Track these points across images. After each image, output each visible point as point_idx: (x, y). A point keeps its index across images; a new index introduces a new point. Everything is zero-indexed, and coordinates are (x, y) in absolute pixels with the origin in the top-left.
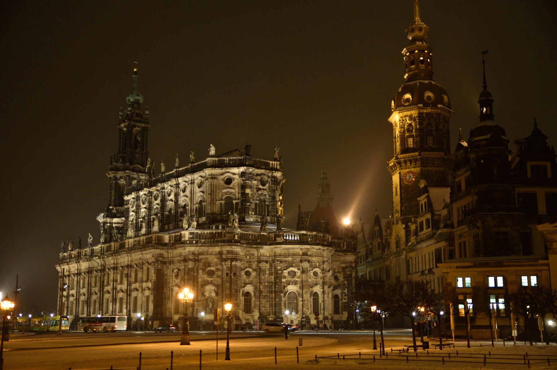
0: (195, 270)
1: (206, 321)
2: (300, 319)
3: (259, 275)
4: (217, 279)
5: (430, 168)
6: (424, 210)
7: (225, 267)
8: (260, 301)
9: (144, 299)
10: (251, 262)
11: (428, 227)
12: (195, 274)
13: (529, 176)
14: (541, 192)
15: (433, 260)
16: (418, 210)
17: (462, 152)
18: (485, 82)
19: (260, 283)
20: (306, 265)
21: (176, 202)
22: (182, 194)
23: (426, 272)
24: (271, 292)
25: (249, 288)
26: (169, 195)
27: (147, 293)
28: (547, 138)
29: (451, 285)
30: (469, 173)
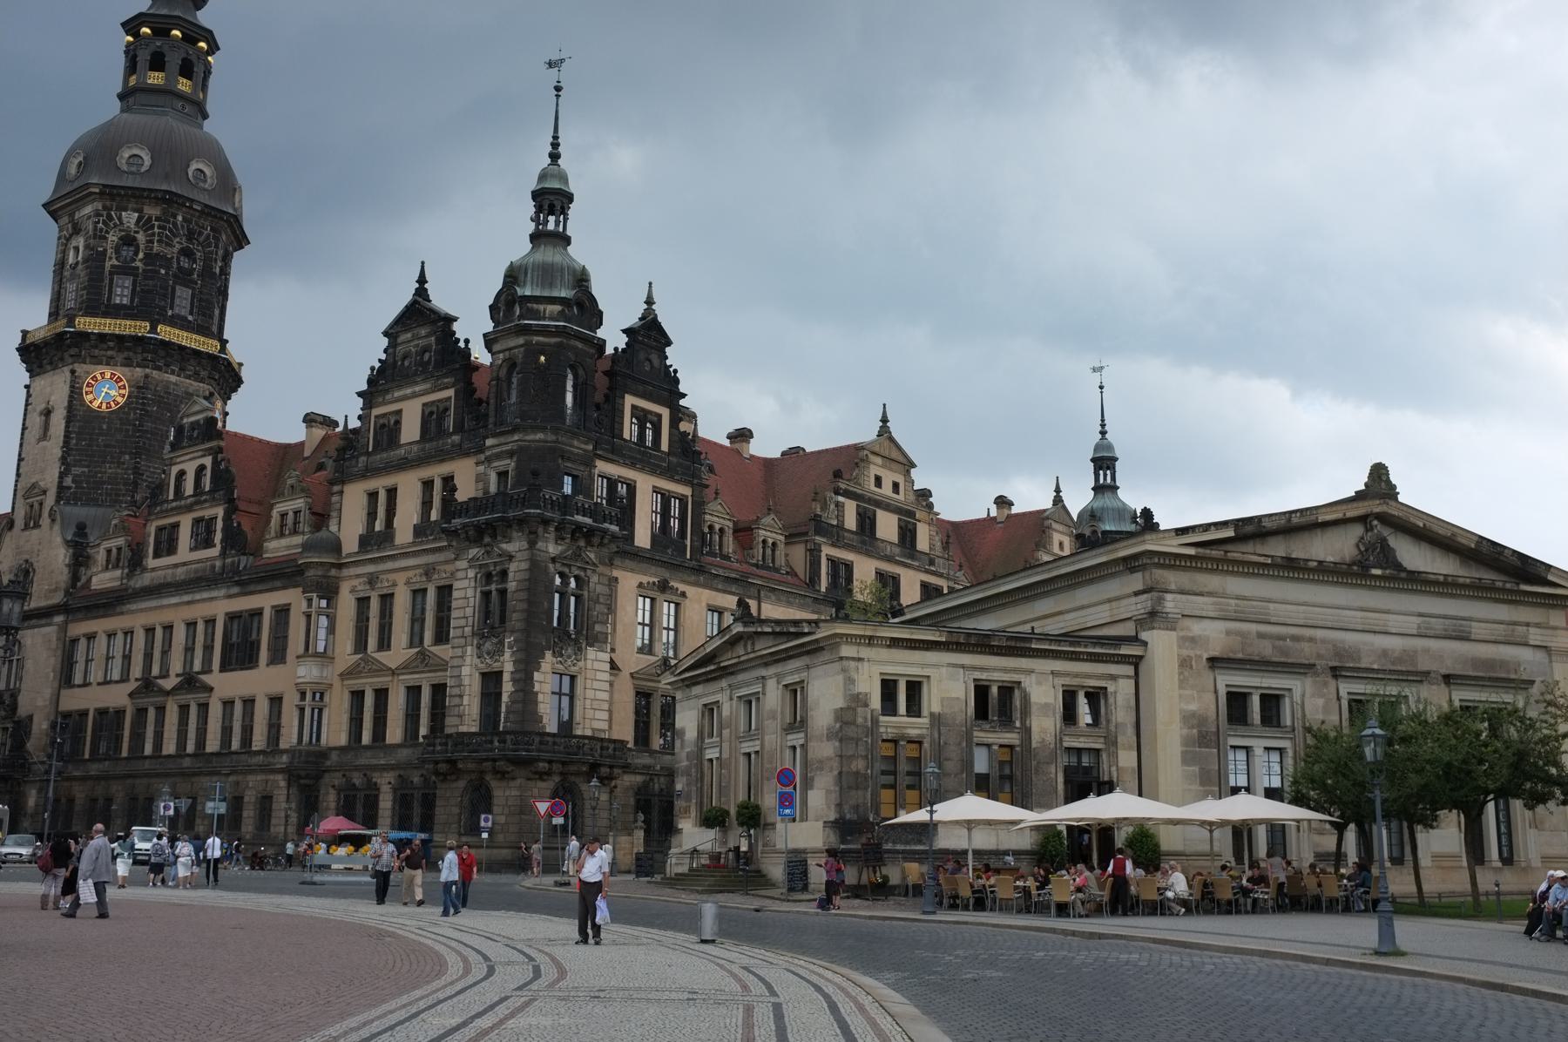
5: (173, 378)
6: (189, 488)
14: (646, 485)
15: (208, 648)
16: (160, 487)
17: (423, 332)
23: (168, 684)
28: (669, 343)
29: (866, 705)
30: (450, 393)
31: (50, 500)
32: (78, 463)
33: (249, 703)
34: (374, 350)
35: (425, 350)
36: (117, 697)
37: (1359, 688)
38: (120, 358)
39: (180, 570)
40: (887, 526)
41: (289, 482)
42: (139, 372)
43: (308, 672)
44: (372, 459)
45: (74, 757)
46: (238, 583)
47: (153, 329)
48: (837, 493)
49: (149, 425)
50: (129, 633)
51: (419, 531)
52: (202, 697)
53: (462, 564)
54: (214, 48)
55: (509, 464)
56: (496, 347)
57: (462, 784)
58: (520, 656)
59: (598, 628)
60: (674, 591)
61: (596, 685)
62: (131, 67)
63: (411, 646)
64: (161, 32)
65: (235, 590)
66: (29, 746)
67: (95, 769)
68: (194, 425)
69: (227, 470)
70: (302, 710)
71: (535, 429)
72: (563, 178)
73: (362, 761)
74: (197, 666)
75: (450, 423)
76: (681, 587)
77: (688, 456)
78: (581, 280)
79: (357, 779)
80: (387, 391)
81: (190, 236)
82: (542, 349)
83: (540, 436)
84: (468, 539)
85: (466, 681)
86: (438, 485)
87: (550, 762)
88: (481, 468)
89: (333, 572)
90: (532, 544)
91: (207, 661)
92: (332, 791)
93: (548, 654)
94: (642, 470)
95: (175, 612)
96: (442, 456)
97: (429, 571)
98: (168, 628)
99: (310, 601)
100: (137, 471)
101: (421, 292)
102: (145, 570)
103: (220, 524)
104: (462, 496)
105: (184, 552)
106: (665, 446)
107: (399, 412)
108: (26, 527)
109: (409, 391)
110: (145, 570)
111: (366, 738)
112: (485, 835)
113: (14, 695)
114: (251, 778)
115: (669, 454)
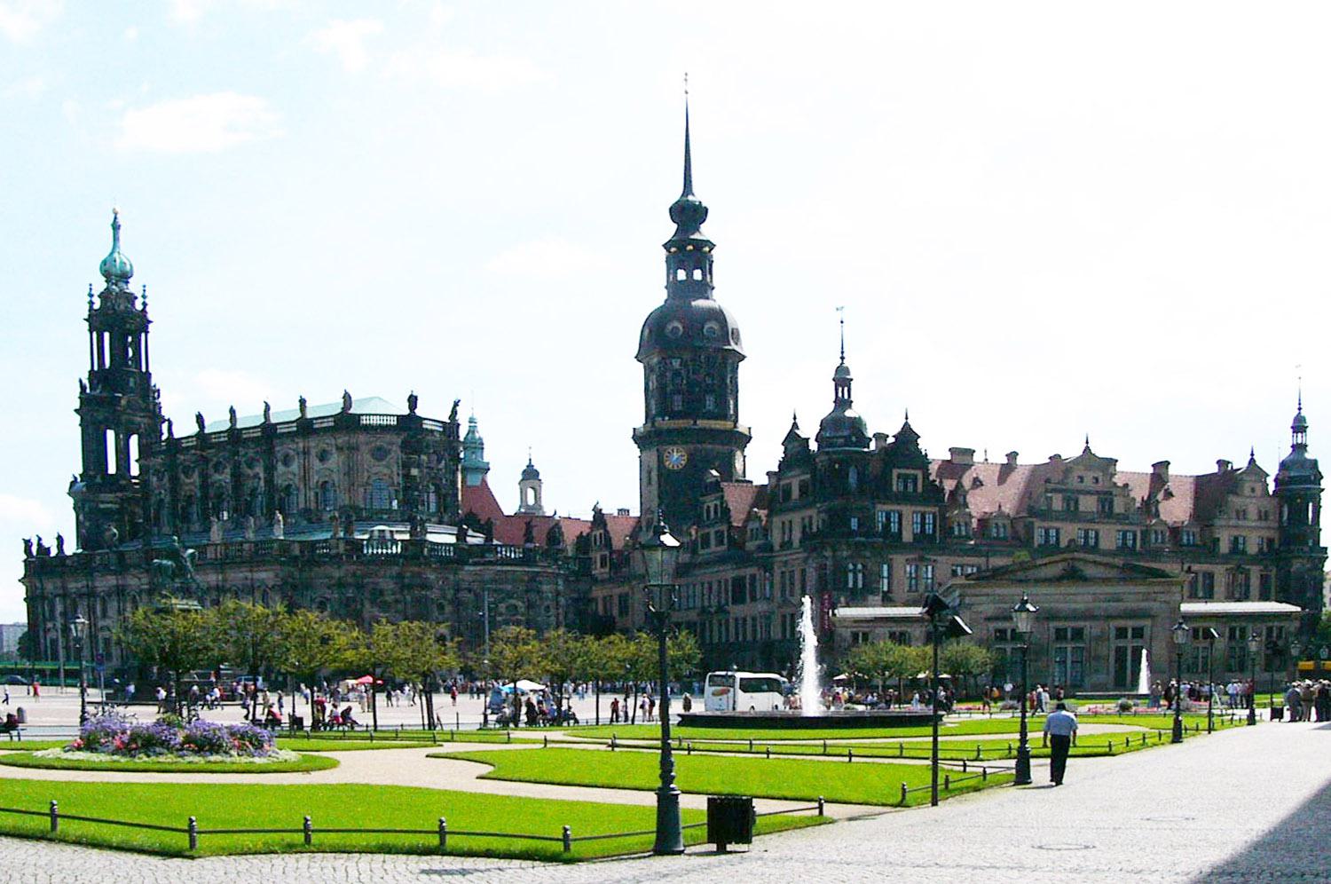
5: (710, 446)
11: (721, 542)
14: (907, 510)
17: (796, 444)
21: (269, 481)
22: (281, 468)
26: (250, 466)
30: (808, 476)
35: (799, 452)
37: (1061, 624)
40: (1088, 504)
42: (692, 447)
48: (1047, 491)
60: (930, 560)
68: (711, 483)
77: (934, 492)
90: (834, 551)
96: (804, 507)
105: (713, 547)
106: (920, 489)
107: (790, 483)
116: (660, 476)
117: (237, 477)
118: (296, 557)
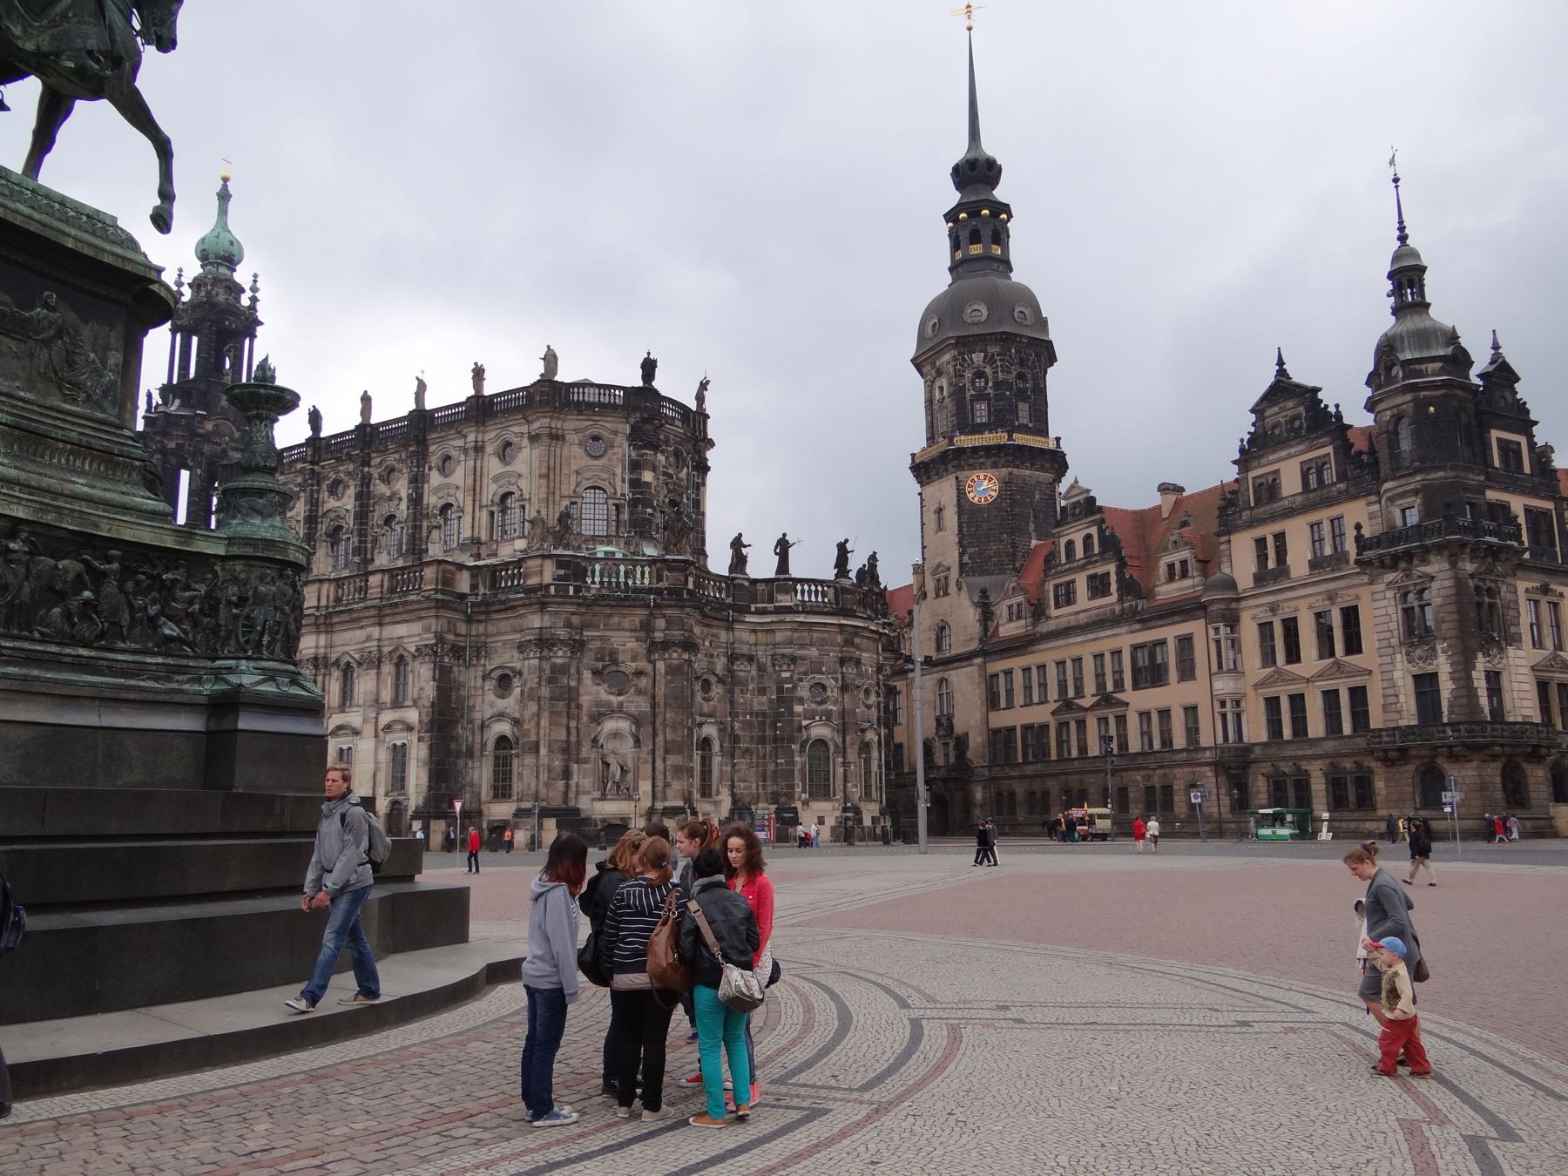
0: (573, 671)
1: (603, 820)
2: (838, 813)
3: (731, 692)
4: (638, 698)
5: (1027, 472)
6: (1079, 553)
7: (661, 665)
8: (734, 765)
9: (384, 756)
10: (712, 656)
12: (573, 684)
13: (1497, 463)
14: (1518, 505)
17: (1290, 404)
18: (1402, 228)
19: (734, 715)
20: (850, 670)
21: (416, 501)
22: (435, 479)
23: (1086, 702)
24: (762, 740)
25: (710, 730)
27: (398, 738)
28: (1517, 379)
30: (1329, 449)
31: (954, 575)
32: (971, 545)
33: (1165, 714)
34: (1244, 425)
35: (1294, 418)
36: (1041, 714)
38: (989, 463)
39: (1082, 616)
41: (1172, 538)
42: (1004, 471)
43: (1224, 685)
44: (1256, 511)
45: (1009, 761)
46: (1139, 621)
47: (1010, 438)
49: (1016, 510)
50: (1042, 668)
51: (1316, 564)
52: (1119, 711)
53: (1381, 587)
54: (1010, 216)
55: (1417, 501)
56: (1380, 407)
57: (1411, 768)
58: (1458, 658)
59: (1513, 630)
61: (1520, 678)
62: (956, 245)
63: (1321, 657)
64: (974, 214)
65: (1137, 626)
66: (969, 754)
67: (1029, 770)
68: (1074, 505)
69: (1113, 535)
70: (1224, 716)
71: (1435, 469)
72: (1415, 254)
73: (1287, 753)
74: (1110, 687)
75: (1330, 475)
76: (1559, 589)
78: (1452, 337)
79: (1286, 767)
80: (1262, 456)
81: (1022, 363)
82: (1430, 401)
83: (1440, 474)
84: (1383, 565)
85: (1400, 683)
86: (1326, 526)
87: (1502, 746)
88: (1376, 507)
89: (1233, 605)
90: (1453, 565)
91: (1119, 685)
92: (1260, 777)
93: (1480, 655)
94: (1513, 492)
95: (1084, 648)
96: (1329, 502)
97: (1331, 597)
98: (1078, 661)
99: (1217, 630)
100: (1014, 545)
101: (1282, 372)
102: (1049, 618)
103: (1113, 578)
104: (1366, 532)
106: (1527, 470)
107: (1277, 472)
108: (937, 596)
109: (1284, 453)
110: (1049, 618)
111: (1287, 733)
112: (1447, 809)
113: (950, 718)
114: (1178, 772)
115: (1532, 475)
116: (960, 513)
117: (364, 497)
118: (463, 596)
